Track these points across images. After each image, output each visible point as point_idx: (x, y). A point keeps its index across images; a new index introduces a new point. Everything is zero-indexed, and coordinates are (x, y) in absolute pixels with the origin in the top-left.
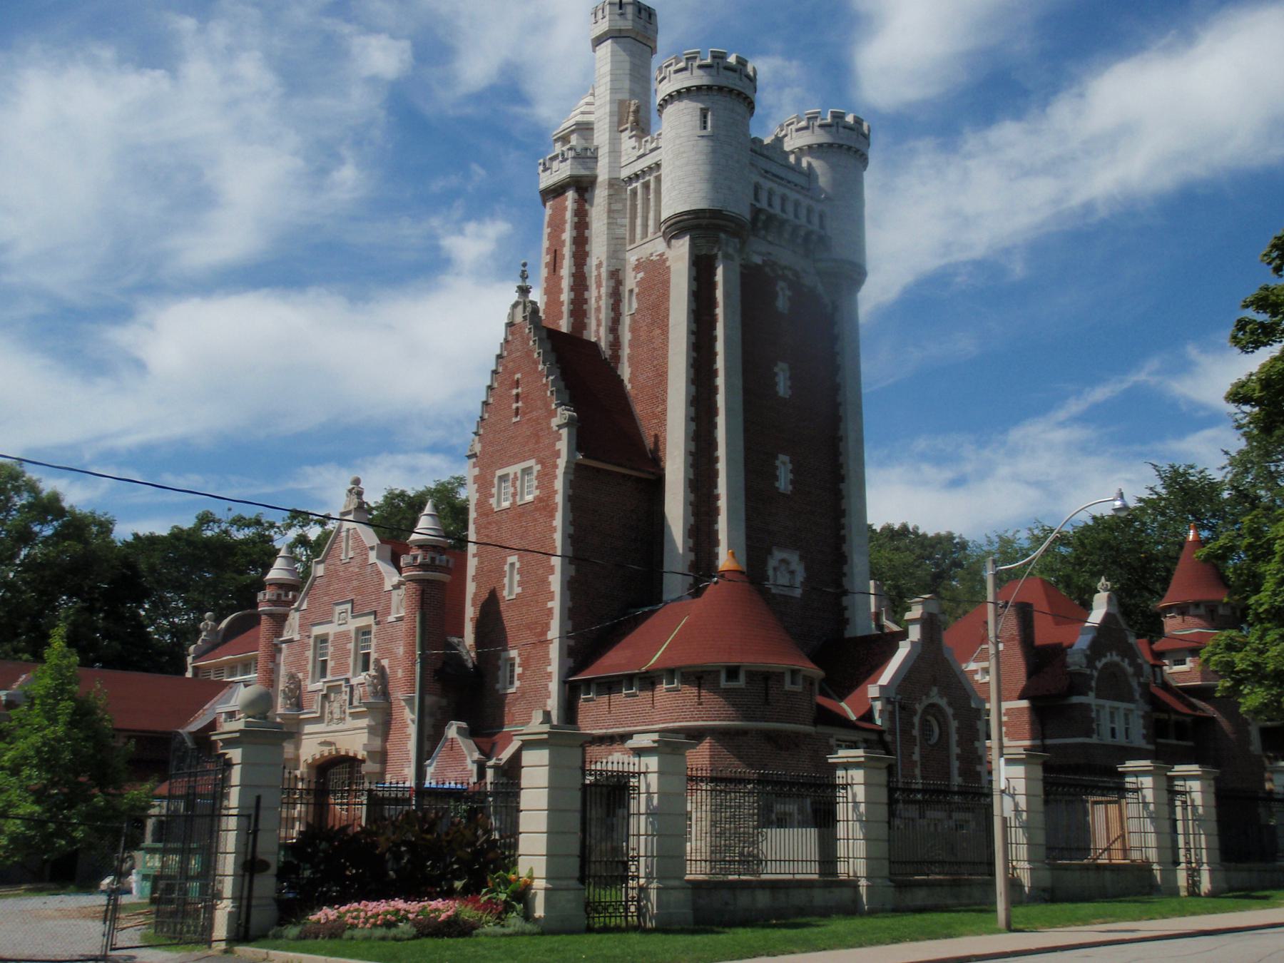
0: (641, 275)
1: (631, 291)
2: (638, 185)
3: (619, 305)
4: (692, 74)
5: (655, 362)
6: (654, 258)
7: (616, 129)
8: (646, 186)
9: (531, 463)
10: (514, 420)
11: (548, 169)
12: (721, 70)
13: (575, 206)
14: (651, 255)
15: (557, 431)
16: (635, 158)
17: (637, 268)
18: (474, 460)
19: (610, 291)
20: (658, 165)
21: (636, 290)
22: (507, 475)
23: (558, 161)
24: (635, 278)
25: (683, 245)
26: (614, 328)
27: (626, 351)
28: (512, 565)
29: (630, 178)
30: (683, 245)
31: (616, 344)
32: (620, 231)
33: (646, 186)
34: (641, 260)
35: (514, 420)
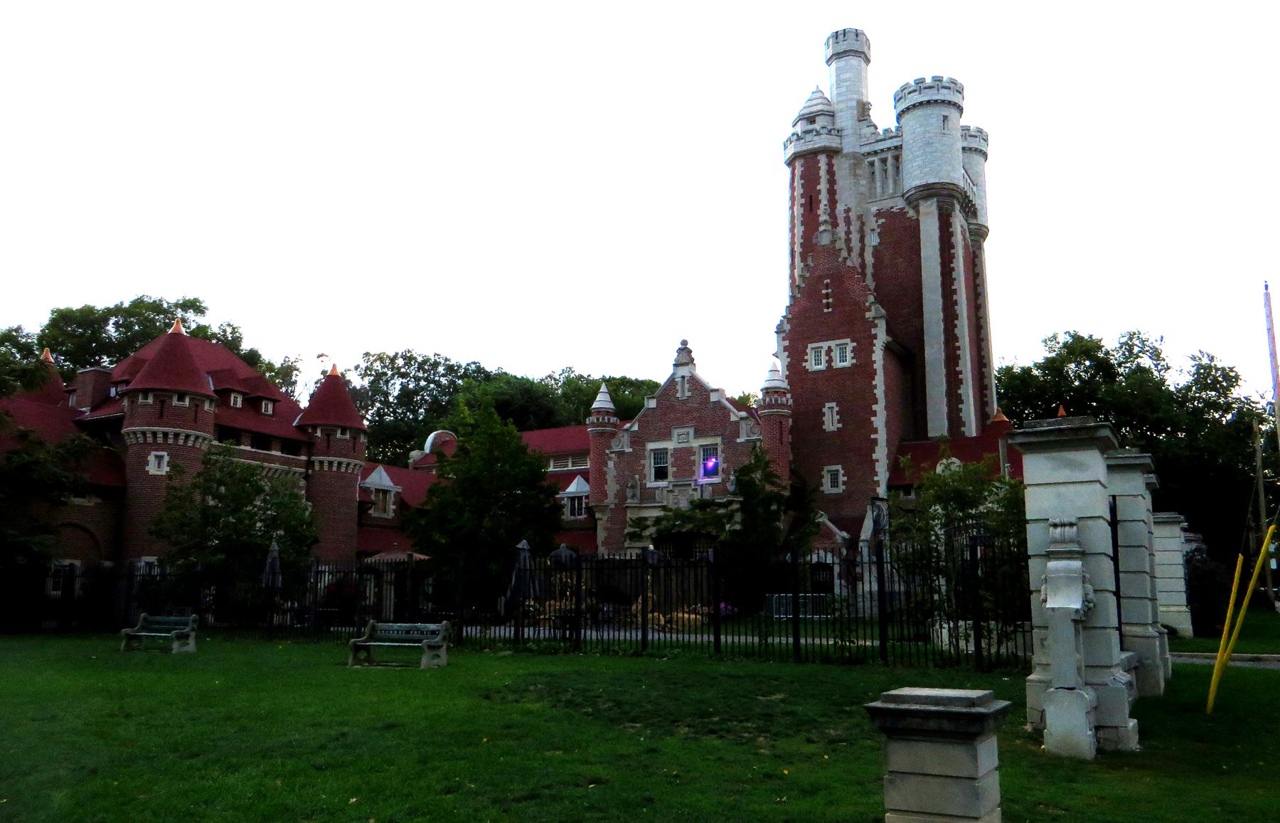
0: (881, 221)
1: (873, 230)
2: (876, 159)
3: (864, 239)
4: (938, 90)
7: (856, 119)
8: (884, 161)
9: (848, 341)
10: (825, 310)
11: (802, 139)
16: (874, 141)
17: (879, 214)
18: (784, 335)
20: (898, 148)
21: (879, 230)
22: (822, 347)
24: (877, 222)
25: (931, 205)
26: (861, 255)
27: (869, 270)
29: (869, 154)
31: (863, 265)
32: (863, 189)
33: (884, 161)
35: (825, 310)
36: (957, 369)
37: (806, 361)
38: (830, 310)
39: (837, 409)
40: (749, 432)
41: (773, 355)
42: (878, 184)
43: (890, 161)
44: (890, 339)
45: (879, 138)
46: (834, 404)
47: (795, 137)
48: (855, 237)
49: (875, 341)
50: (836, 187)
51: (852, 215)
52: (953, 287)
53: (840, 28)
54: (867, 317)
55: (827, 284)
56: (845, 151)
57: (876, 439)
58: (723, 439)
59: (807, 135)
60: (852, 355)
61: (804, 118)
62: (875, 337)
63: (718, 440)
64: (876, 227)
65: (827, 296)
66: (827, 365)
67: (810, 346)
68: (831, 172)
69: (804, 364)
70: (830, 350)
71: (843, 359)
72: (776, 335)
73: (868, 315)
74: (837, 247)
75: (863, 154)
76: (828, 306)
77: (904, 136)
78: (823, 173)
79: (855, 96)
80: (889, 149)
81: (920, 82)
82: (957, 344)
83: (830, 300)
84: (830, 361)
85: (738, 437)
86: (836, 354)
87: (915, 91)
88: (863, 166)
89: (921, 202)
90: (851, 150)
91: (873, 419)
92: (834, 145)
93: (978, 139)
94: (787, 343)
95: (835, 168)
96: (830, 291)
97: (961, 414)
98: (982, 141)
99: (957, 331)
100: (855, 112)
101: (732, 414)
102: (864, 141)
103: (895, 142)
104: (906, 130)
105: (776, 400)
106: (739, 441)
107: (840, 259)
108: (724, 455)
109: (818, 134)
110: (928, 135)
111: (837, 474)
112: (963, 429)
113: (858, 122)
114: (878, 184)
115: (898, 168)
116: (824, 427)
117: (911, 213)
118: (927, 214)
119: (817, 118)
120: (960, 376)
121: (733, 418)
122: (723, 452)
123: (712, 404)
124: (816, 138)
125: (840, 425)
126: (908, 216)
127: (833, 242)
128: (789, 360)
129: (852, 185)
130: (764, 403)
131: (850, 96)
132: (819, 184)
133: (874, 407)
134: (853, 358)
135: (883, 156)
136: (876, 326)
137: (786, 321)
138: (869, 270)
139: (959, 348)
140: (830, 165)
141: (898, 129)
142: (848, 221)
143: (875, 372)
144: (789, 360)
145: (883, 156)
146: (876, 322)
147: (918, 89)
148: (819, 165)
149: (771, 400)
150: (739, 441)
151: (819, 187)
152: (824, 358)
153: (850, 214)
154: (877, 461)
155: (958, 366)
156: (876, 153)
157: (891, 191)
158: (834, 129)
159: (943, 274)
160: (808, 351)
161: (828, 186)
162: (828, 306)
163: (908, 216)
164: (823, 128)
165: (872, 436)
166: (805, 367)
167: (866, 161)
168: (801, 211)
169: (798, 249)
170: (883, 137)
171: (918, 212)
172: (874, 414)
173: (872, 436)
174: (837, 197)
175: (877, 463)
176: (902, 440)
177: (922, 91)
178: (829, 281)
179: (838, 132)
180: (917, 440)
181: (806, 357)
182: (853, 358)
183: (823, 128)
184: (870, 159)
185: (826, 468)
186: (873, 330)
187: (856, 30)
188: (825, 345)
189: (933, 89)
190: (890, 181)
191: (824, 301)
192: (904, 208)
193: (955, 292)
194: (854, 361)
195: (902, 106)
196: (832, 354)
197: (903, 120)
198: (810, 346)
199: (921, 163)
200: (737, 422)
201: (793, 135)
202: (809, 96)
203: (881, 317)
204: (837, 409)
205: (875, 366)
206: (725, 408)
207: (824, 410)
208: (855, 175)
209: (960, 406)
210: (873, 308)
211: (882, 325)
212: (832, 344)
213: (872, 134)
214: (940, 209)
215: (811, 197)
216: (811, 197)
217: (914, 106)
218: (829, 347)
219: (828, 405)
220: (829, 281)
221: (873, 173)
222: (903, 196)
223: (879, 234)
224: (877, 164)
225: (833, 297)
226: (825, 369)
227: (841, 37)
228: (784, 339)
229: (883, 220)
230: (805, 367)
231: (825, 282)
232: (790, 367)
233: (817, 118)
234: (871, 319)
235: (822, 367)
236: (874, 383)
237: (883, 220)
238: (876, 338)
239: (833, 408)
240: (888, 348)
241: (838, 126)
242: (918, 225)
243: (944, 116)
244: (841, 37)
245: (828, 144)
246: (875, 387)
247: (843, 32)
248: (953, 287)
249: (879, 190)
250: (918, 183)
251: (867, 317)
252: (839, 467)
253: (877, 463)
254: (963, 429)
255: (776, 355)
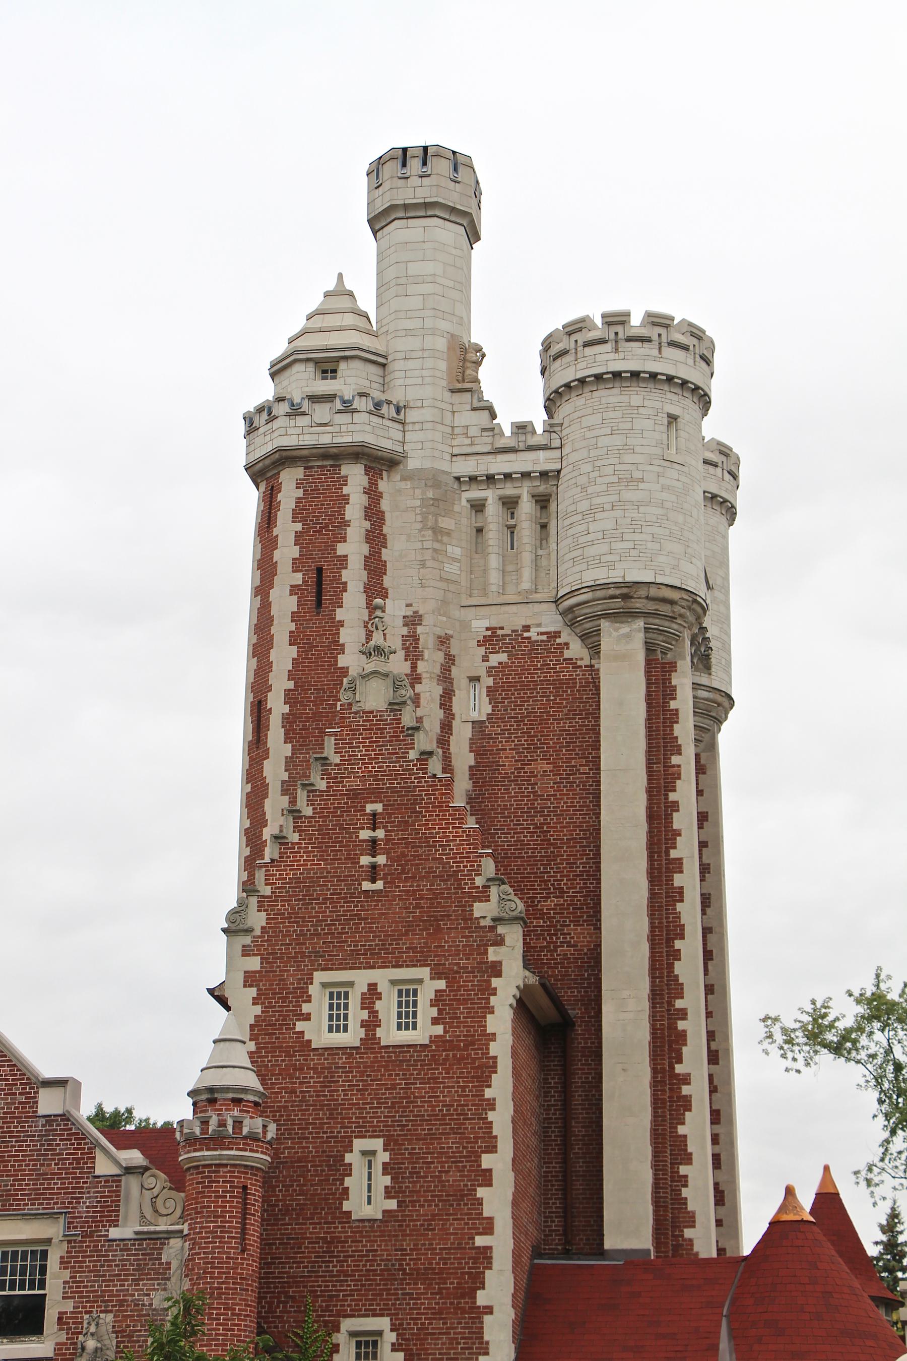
0: (496, 659)
1: (475, 679)
2: (490, 495)
3: (450, 699)
5: (539, 820)
6: (533, 634)
7: (444, 383)
8: (510, 504)
9: (424, 972)
10: (366, 886)
11: (304, 414)
12: (698, 358)
13: (364, 500)
14: (527, 628)
15: (493, 928)
16: (487, 449)
18: (247, 940)
19: (437, 670)
21: (490, 682)
22: (351, 984)
23: (327, 406)
24: (485, 659)
25: (628, 636)
26: (444, 741)
28: (369, 1154)
29: (473, 479)
30: (628, 636)
31: (447, 767)
32: (452, 569)
33: (510, 504)
34: (499, 632)
35: (366, 886)
36: (679, 1069)
37: (307, 1017)
38: (379, 885)
39: (384, 1157)
40: (148, 1212)
41: (211, 991)
42: (494, 561)
43: (526, 507)
44: (533, 980)
45: (501, 443)
46: (377, 1144)
47: (284, 408)
48: (430, 691)
49: (495, 982)
50: (385, 554)
51: (426, 633)
52: (674, 854)
53: (414, 140)
54: (476, 914)
55: (374, 815)
56: (413, 463)
57: (490, 1248)
58: (69, 1225)
59: (317, 406)
60: (434, 1012)
61: (308, 360)
62: (496, 969)
63: (52, 1230)
64: (483, 672)
65: (373, 846)
66: (362, 1033)
67: (319, 977)
68: (374, 514)
69: (300, 1026)
70: (372, 994)
71: (407, 1021)
72: (224, 937)
73: (479, 909)
74: (407, 719)
75: (458, 479)
76: (373, 873)
77: (566, 450)
78: (354, 511)
79: (444, 325)
80: (526, 475)
81: (615, 320)
82: (679, 1004)
83: (381, 860)
84: (371, 1024)
85: (115, 1223)
86: (388, 1008)
87: (602, 341)
88: (457, 508)
89: (605, 624)
90: (427, 464)
91: (481, 1192)
92: (387, 444)
93: (719, 470)
94: (254, 963)
95: (385, 505)
96: (380, 834)
97: (685, 1192)
98: (727, 477)
99: (679, 968)
100: (443, 365)
101: (100, 1157)
102: (461, 444)
103: (542, 461)
104: (573, 433)
105: (238, 1124)
106: (114, 1233)
107: (412, 755)
108: (66, 1275)
109: (348, 408)
110: (628, 458)
111: (375, 1343)
112: (688, 1233)
113: (448, 394)
114: (494, 561)
115: (544, 526)
116: (346, 1206)
117: (576, 650)
118: (619, 657)
119: (342, 366)
120: (685, 1090)
121: (103, 1167)
122: (64, 1263)
123: (42, 1121)
124: (345, 418)
125: (392, 1204)
126: (567, 654)
127: (396, 706)
128: (258, 1010)
129: (428, 555)
130: (204, 1131)
131: (429, 323)
132: (344, 539)
133: (487, 1160)
134: (435, 1021)
135: (509, 490)
136: (499, 942)
137: (253, 901)
138: (462, 785)
139: (683, 1014)
140: (373, 494)
141: (550, 429)
142: (412, 651)
143: (492, 1066)
144: (258, 1010)
145: (509, 490)
146: (500, 930)
147: (612, 336)
148: (345, 490)
149: (222, 1124)
150: (114, 1233)
151: (341, 549)
152: (356, 1014)
153: (420, 629)
154: (489, 1310)
155: (680, 1061)
156: (490, 478)
157: (526, 585)
158: (389, 403)
159: (651, 816)
160: (313, 990)
161: (365, 549)
162: (373, 873)
163: (567, 654)
164: (362, 395)
165: (480, 1241)
166: (303, 1032)
167: (466, 495)
168: (292, 603)
169: (277, 706)
170: (512, 443)
171: (595, 650)
172: (486, 1178)
173: (480, 1241)
174: (387, 581)
175: (487, 1319)
176: (537, 1253)
177: (623, 345)
178: (379, 807)
179: (398, 411)
180: (567, 1253)
181: (306, 1008)
182: (435, 1021)
183: (362, 395)
184: (476, 493)
185: (348, 1324)
186: (491, 950)
187: (454, 153)
188: (361, 978)
189: (646, 345)
190: (527, 557)
191: (365, 860)
192: (557, 634)
193: (677, 865)
194: (439, 1030)
195: (566, 373)
196: (378, 1005)
197: (565, 410)
198: (319, 977)
199: (609, 525)
200: (116, 1178)
201: (279, 399)
202: (315, 301)
203: (516, 919)
204: (384, 1157)
205: (494, 1049)
206: (81, 1137)
207: (348, 1158)
208: (438, 532)
209: (683, 1170)
210: (494, 891)
211: (514, 936)
212: (382, 977)
213: (484, 430)
214: (650, 648)
215: (320, 571)
216: (320, 571)
217: (598, 377)
218: (373, 987)
219: (359, 1144)
220: (379, 807)
221: (479, 531)
222: (556, 602)
223: (490, 691)
224: (493, 509)
225: (387, 852)
226: (357, 1044)
227: (414, 165)
228: (246, 952)
229: (503, 657)
230: (303, 1032)
231: (369, 808)
232: (258, 1030)
233: (342, 366)
234: (486, 922)
235: (352, 1037)
236: (488, 1093)
237: (503, 657)
238: (499, 974)
239: (373, 1153)
240: (523, 1007)
241: (397, 395)
242: (595, 686)
243: (670, 416)
244: (414, 165)
245: (370, 439)
246: (491, 1105)
247: (420, 152)
248: (674, 854)
249: (494, 577)
250: (601, 575)
251: (476, 914)
252: (383, 1323)
253: (487, 1319)
254: (688, 1233)
255: (219, 996)
